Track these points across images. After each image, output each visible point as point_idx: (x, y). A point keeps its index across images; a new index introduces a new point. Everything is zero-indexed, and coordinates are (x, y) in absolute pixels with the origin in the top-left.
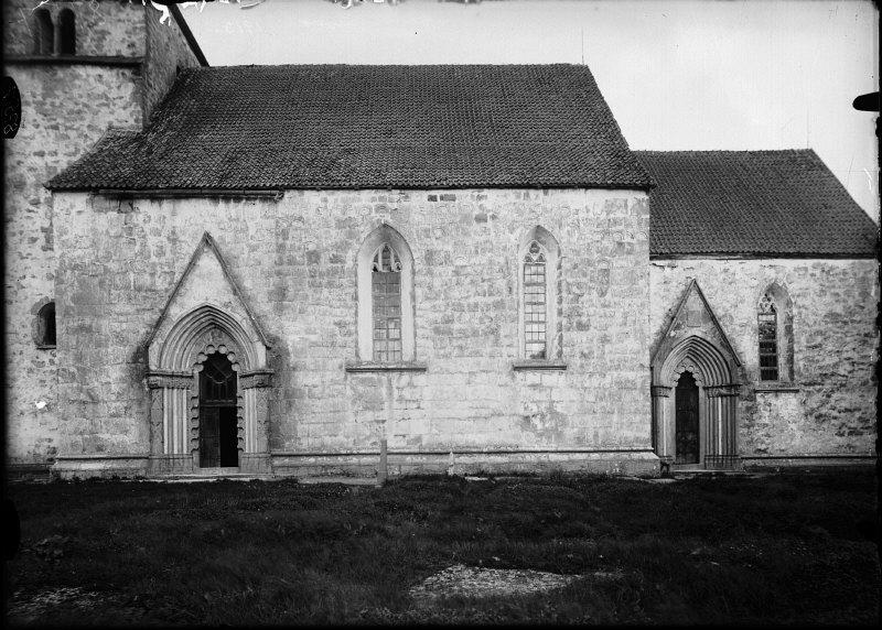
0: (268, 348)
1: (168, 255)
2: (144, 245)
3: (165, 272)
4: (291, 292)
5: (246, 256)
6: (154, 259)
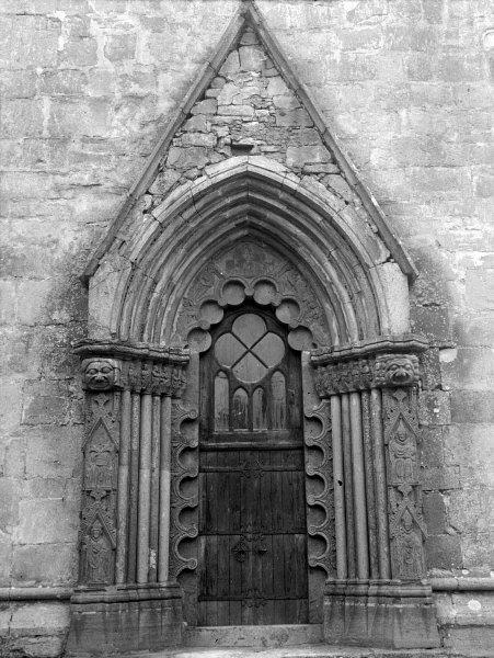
0: (411, 279)
1: (144, 57)
2: (81, 35)
3: (132, 96)
4: (453, 146)
5: (337, 55)
6: (104, 64)
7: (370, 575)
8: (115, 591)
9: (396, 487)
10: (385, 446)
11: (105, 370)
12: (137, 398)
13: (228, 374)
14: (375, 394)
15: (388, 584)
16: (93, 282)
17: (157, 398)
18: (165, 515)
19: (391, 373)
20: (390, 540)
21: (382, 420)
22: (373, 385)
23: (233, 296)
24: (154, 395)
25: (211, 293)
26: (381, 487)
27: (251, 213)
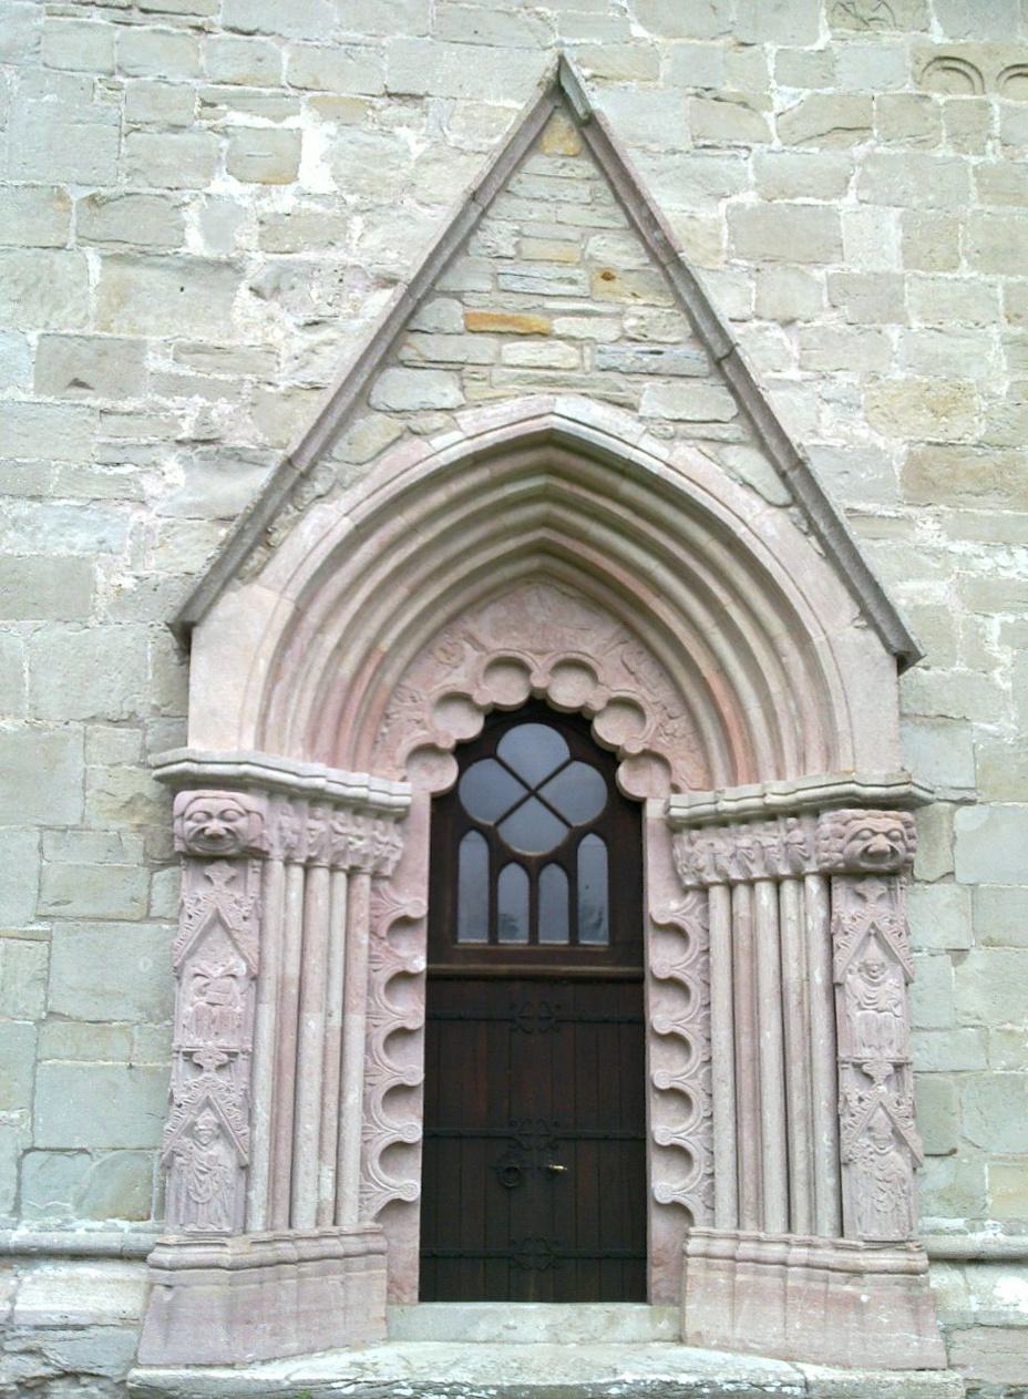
7: (790, 1228)
8: (245, 1248)
9: (858, 1066)
10: (833, 987)
11: (230, 814)
12: (297, 873)
13: (489, 835)
14: (813, 884)
15: (837, 1248)
16: (200, 637)
17: (341, 877)
18: (353, 1098)
19: (858, 846)
20: (840, 1165)
21: (830, 939)
22: (811, 867)
23: (509, 692)
24: (333, 869)
25: (458, 680)
26: (823, 1064)
27: (546, 522)
